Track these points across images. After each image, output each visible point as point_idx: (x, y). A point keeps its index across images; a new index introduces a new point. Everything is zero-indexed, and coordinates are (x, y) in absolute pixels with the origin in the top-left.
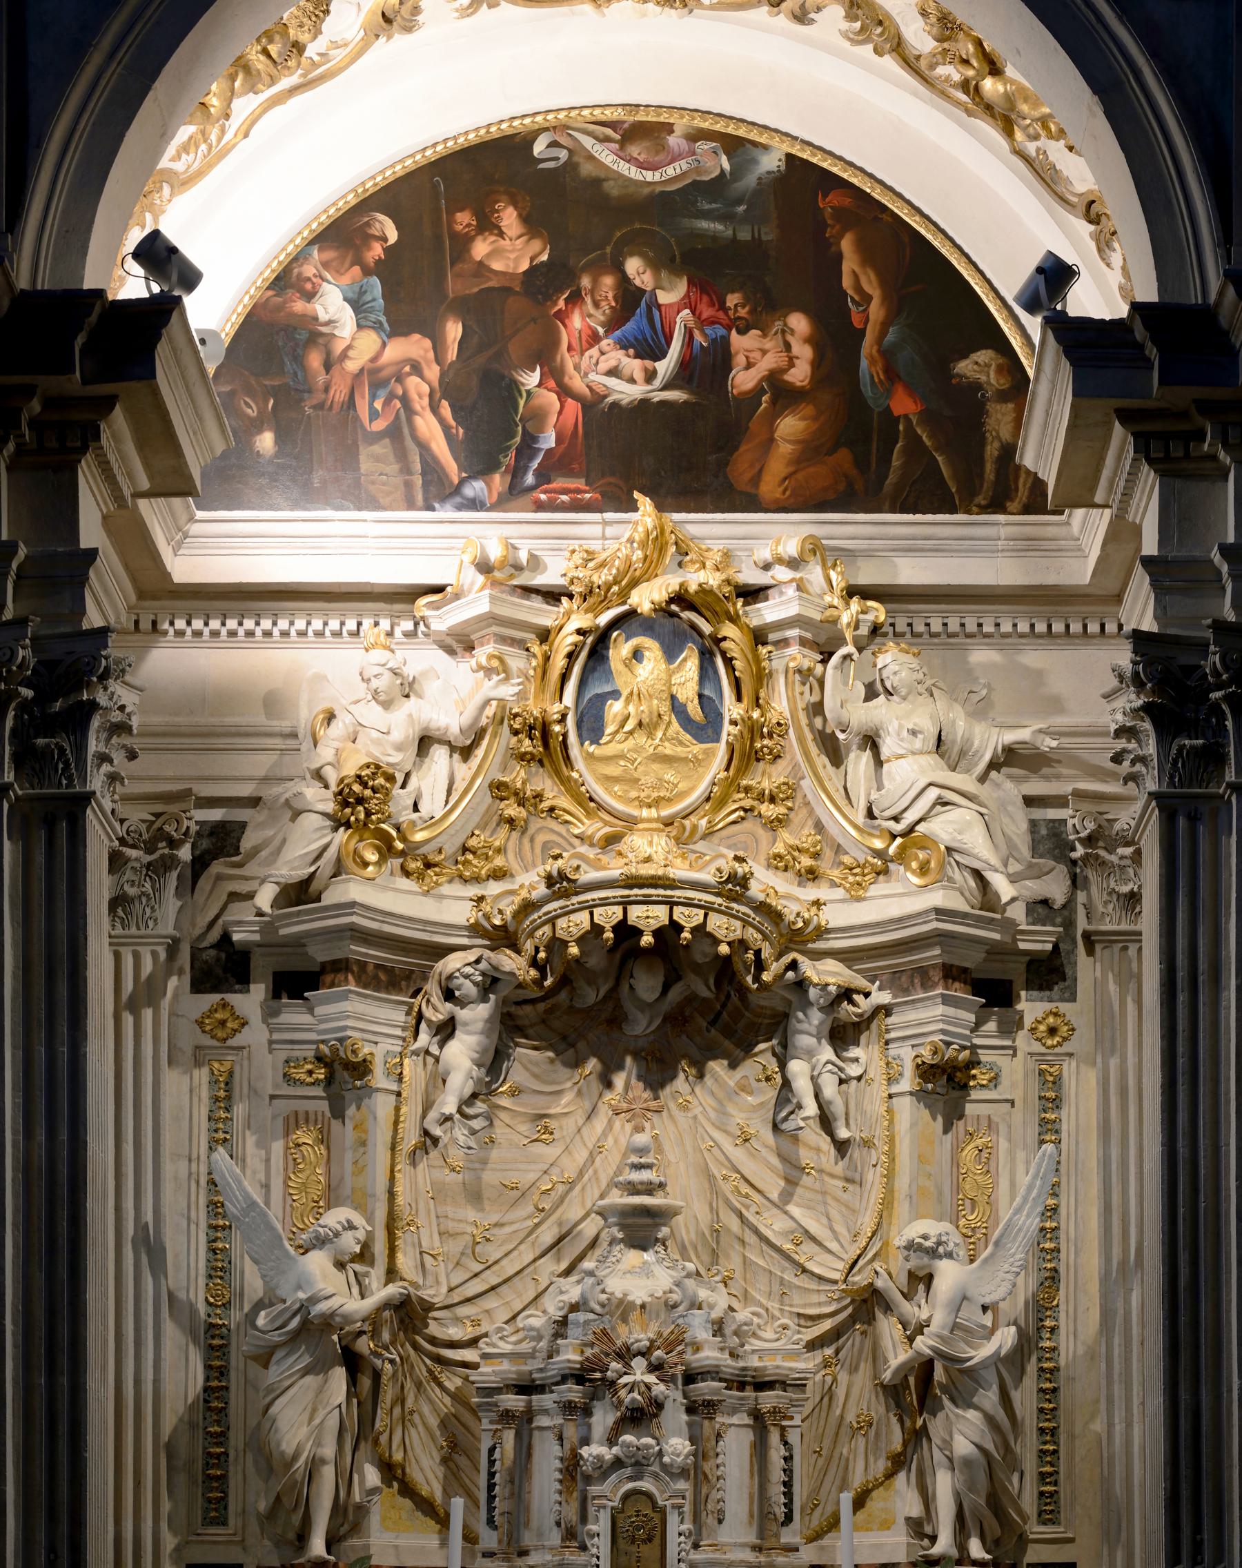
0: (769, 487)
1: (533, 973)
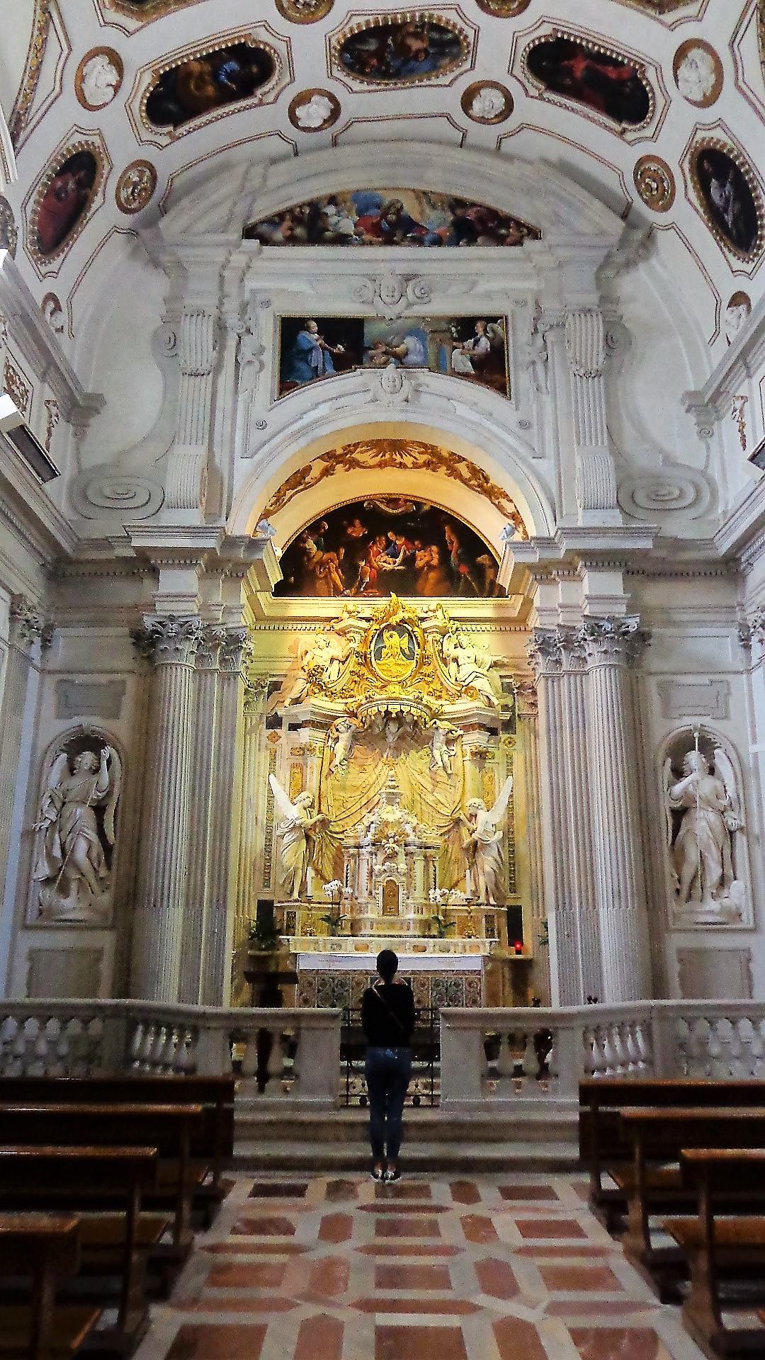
0: (426, 591)
1: (361, 724)
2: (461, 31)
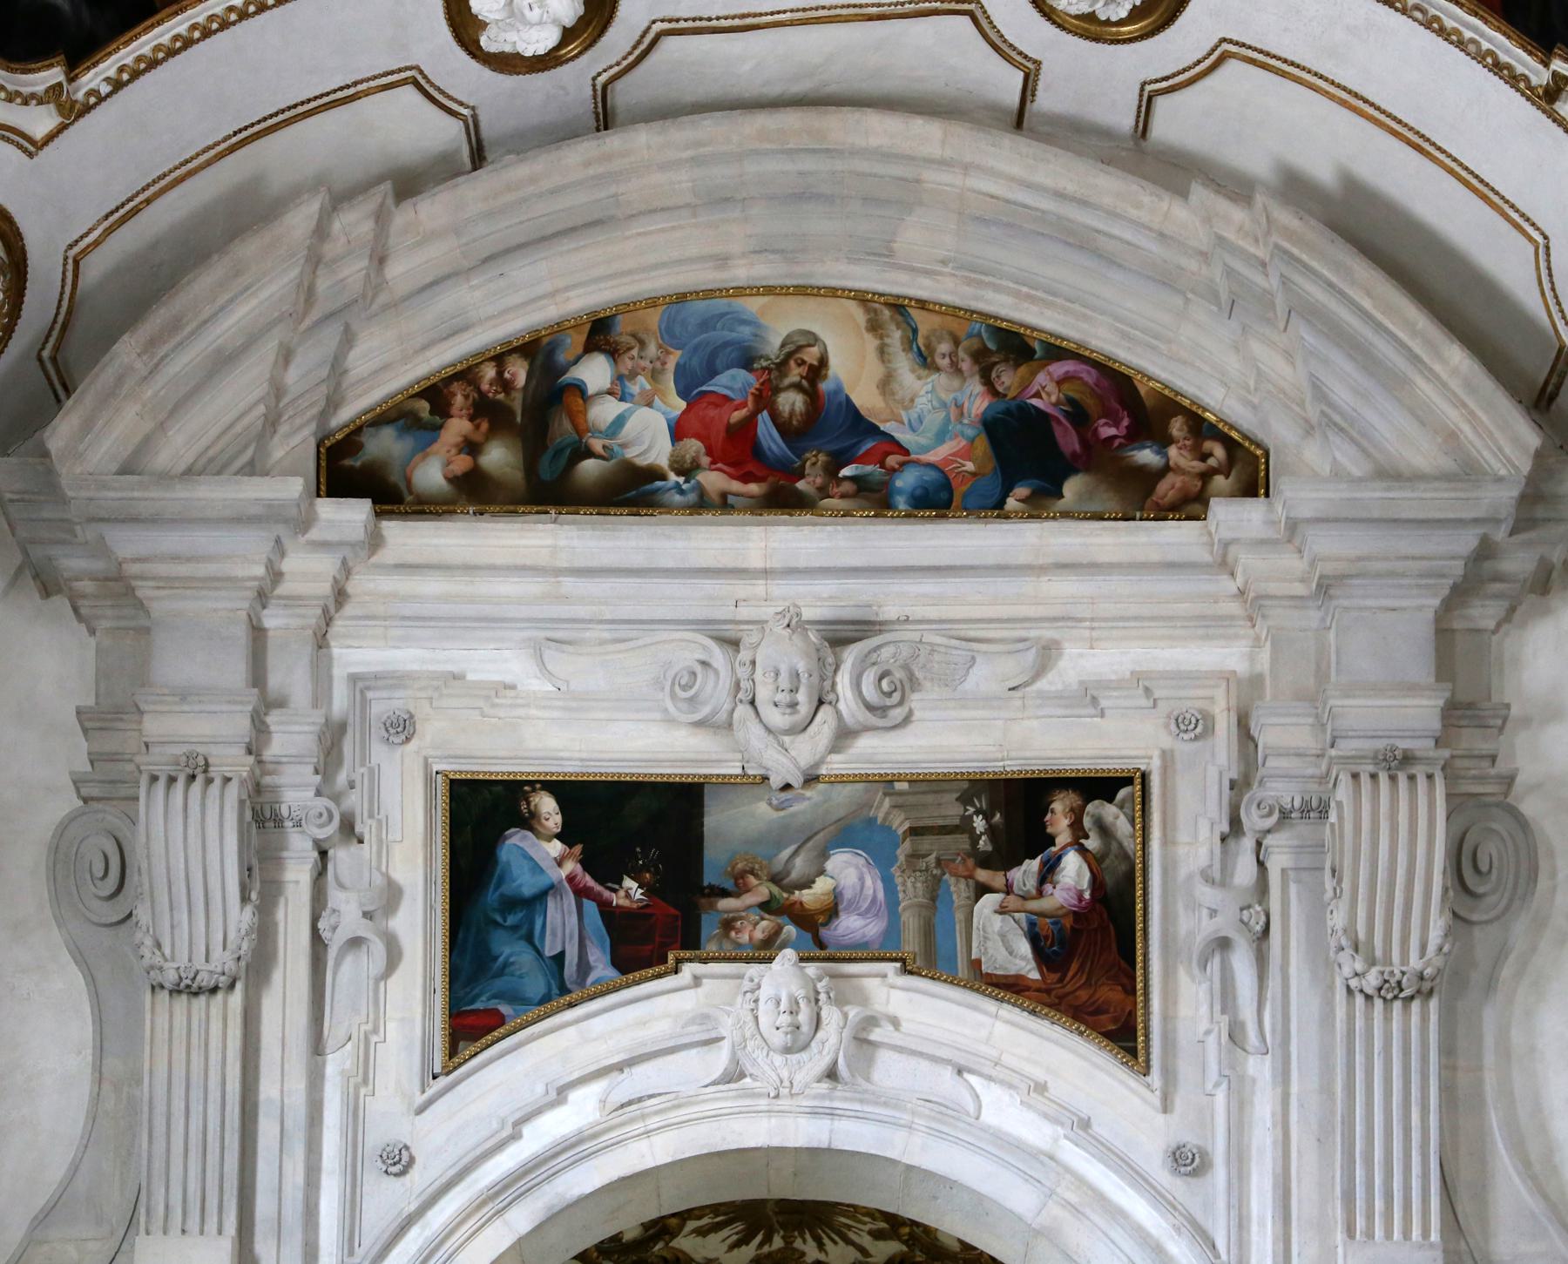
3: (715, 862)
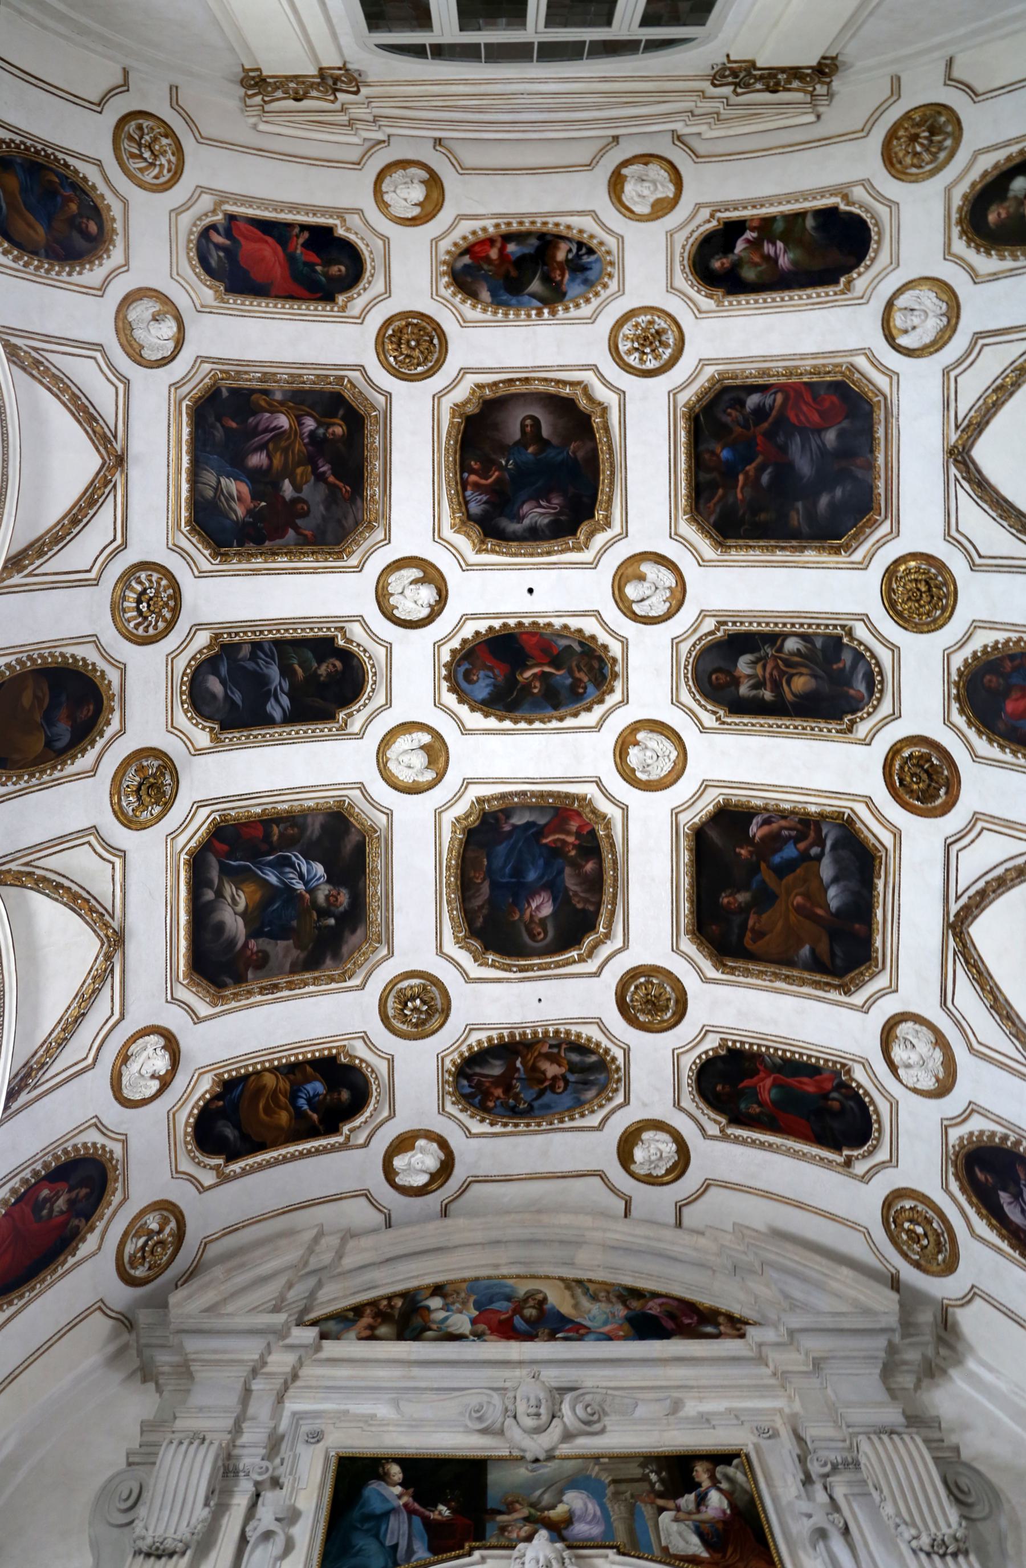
2: (607, 1051)
3: (494, 1497)
